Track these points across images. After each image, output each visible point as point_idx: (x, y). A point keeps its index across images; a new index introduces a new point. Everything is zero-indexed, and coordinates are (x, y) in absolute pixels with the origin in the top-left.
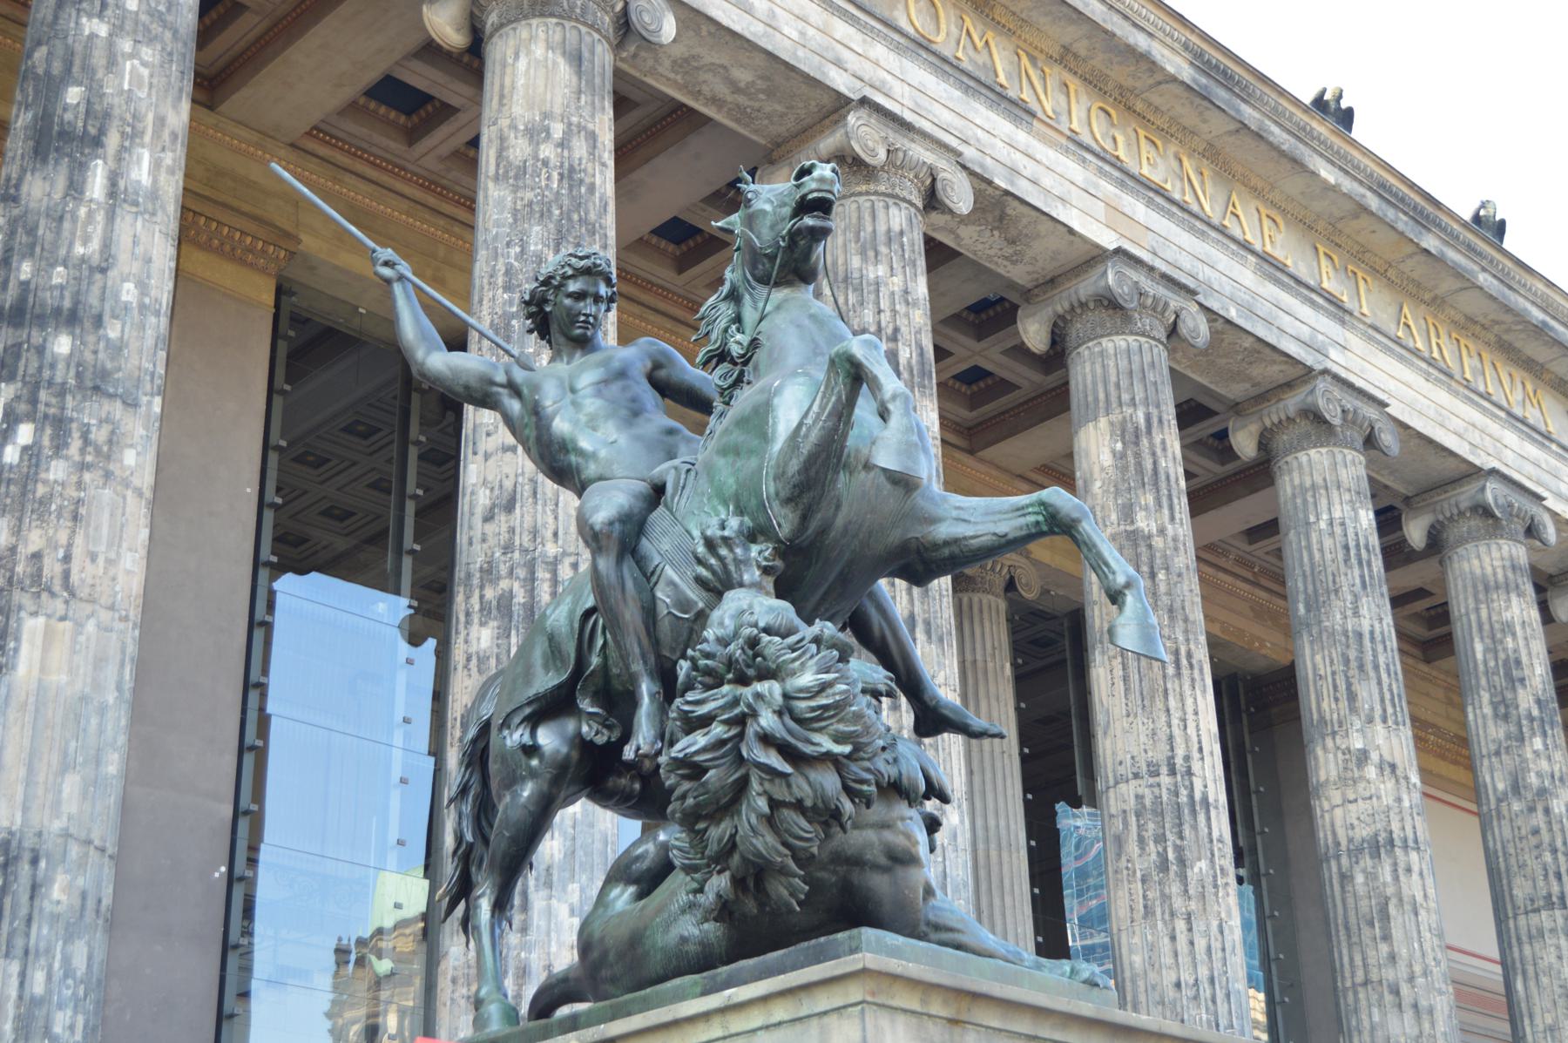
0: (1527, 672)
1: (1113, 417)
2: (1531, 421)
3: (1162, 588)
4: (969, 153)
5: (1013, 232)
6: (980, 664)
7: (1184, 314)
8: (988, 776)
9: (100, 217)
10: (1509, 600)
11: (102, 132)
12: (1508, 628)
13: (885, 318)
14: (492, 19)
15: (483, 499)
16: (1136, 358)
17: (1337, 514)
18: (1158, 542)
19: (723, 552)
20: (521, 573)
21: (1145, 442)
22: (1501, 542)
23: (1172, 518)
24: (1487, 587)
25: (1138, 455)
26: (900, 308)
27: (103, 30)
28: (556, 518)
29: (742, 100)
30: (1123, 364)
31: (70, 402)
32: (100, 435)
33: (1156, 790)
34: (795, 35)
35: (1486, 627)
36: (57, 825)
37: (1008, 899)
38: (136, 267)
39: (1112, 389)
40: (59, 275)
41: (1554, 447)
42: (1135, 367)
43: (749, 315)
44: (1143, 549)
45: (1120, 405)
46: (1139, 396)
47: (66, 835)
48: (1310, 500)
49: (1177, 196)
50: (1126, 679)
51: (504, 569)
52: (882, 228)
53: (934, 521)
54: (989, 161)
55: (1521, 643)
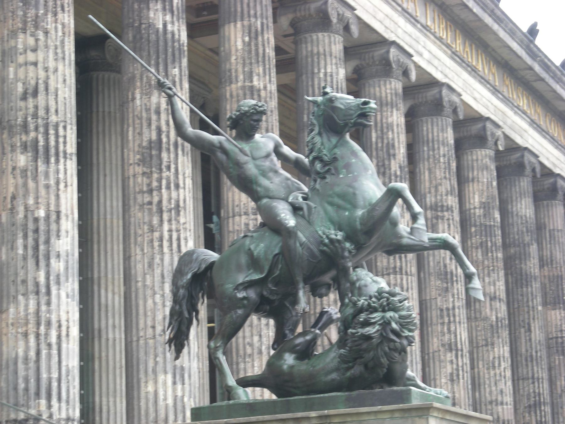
0: (397, 151)
1: (246, 23)
2: (410, 11)
6: (113, 114)
10: (392, 112)
12: (390, 127)
15: (20, 88)
17: (329, 70)
19: (337, 245)
20: (41, 129)
21: (260, 38)
22: (392, 80)
25: (257, 45)
28: (57, 103)
33: (255, 222)
35: (379, 125)
39: (245, 6)
41: (419, 26)
45: (249, 16)
46: (259, 13)
48: (316, 60)
51: (32, 127)
53: (401, 237)
55: (396, 135)
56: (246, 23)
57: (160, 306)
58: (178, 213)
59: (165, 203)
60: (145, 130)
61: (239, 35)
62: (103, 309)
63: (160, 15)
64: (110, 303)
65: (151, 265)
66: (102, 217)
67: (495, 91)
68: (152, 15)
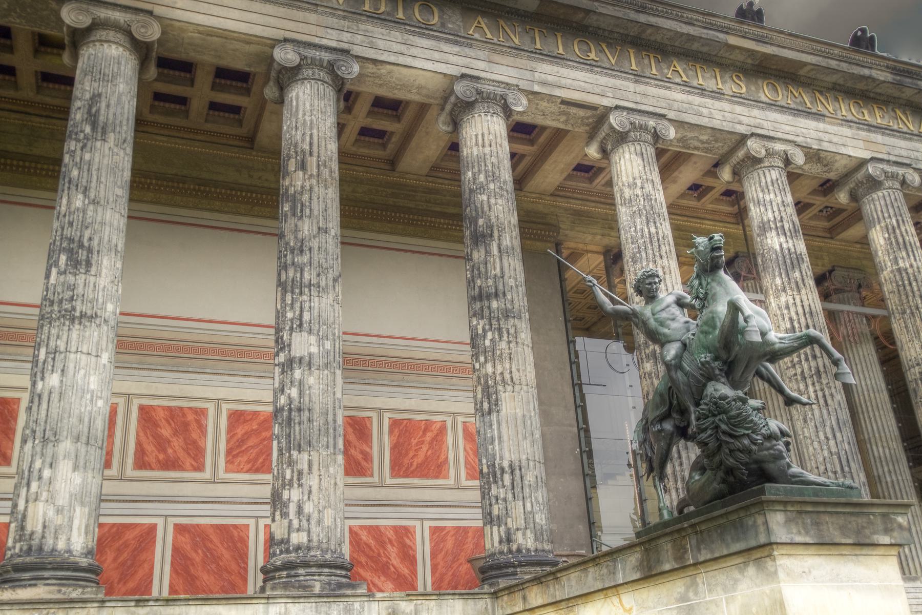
1: (883, 224)
3: (915, 289)
4: (799, 140)
5: (825, 162)
7: (907, 175)
8: (864, 364)
9: (498, 260)
11: (492, 232)
13: (777, 214)
14: (609, 147)
16: (888, 199)
18: (910, 271)
21: (898, 231)
23: (915, 260)
25: (896, 237)
26: (782, 209)
27: (485, 198)
29: (705, 145)
30: (882, 202)
31: (501, 323)
32: (512, 331)
34: (721, 118)
36: (524, 457)
37: (882, 412)
38: (512, 273)
39: (879, 213)
40: (490, 282)
42: (888, 202)
43: (704, 283)
44: (904, 274)
45: (884, 219)
46: (892, 213)
47: (528, 459)
49: (896, 127)
50: (906, 327)
52: (769, 180)
53: (773, 344)
54: (809, 140)
56: (883, 224)
57: (819, 451)
58: (820, 377)
59: (806, 372)
60: (782, 323)
61: (880, 235)
62: (878, 460)
63: (776, 239)
64: (882, 454)
65: (805, 421)
66: (861, 394)
68: (769, 241)
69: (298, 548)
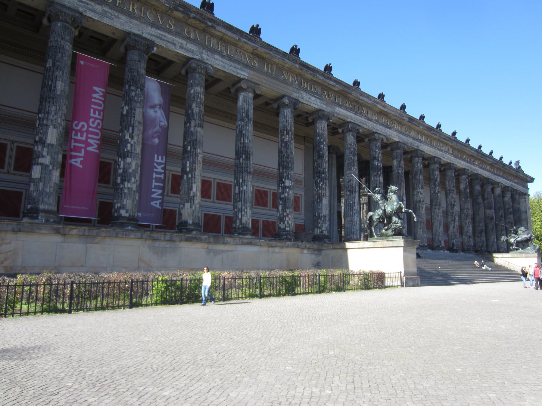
24: (434, 170)
67: (468, 162)
69: (287, 231)
